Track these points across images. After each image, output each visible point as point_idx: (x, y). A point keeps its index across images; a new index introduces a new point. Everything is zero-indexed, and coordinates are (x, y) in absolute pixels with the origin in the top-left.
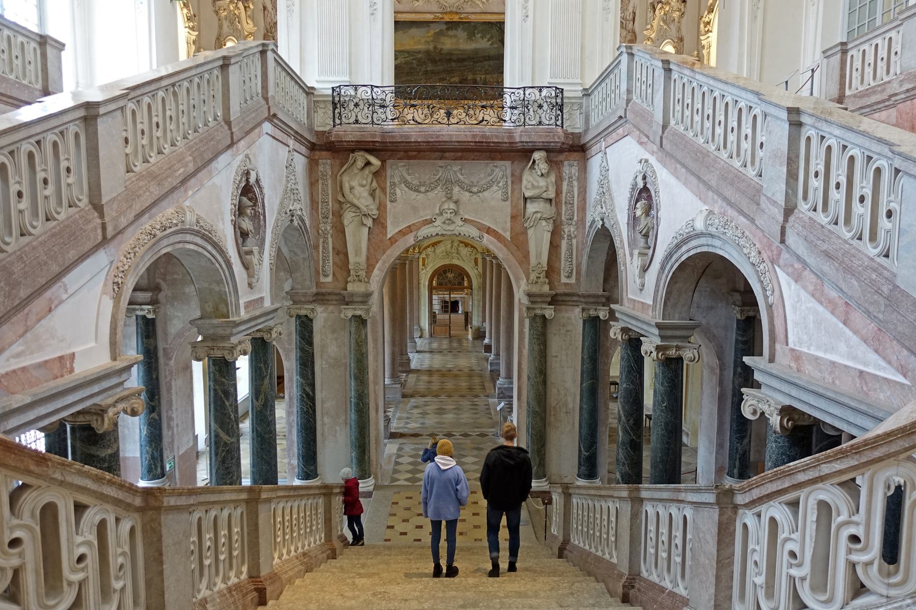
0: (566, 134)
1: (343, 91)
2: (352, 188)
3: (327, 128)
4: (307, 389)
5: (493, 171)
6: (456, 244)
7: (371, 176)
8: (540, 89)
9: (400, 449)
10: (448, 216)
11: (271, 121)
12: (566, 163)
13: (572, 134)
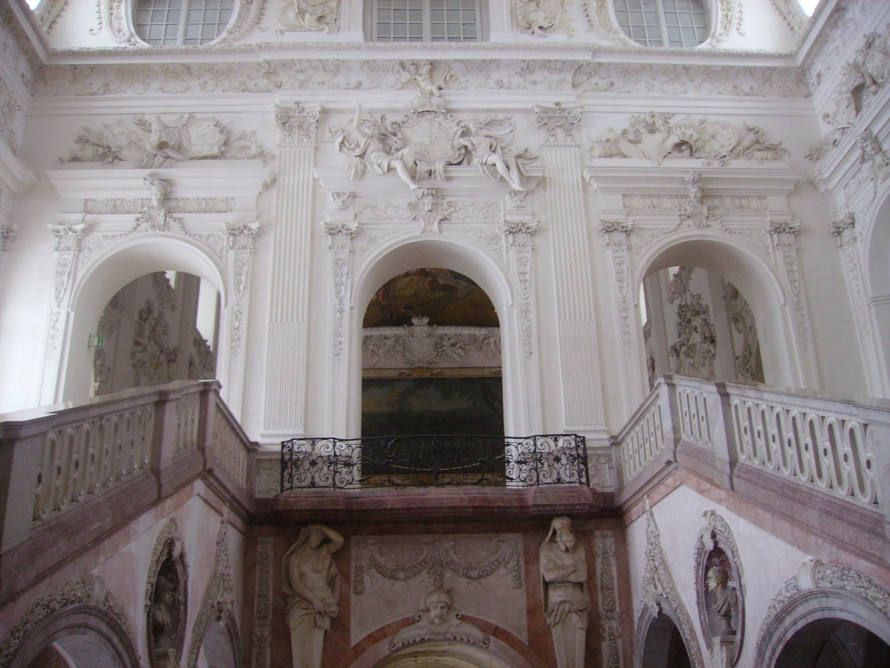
0: (595, 493)
1: (295, 447)
2: (302, 575)
3: (272, 495)
5: (499, 547)
8: (556, 438)
11: (205, 479)
12: (597, 533)
13: (602, 493)
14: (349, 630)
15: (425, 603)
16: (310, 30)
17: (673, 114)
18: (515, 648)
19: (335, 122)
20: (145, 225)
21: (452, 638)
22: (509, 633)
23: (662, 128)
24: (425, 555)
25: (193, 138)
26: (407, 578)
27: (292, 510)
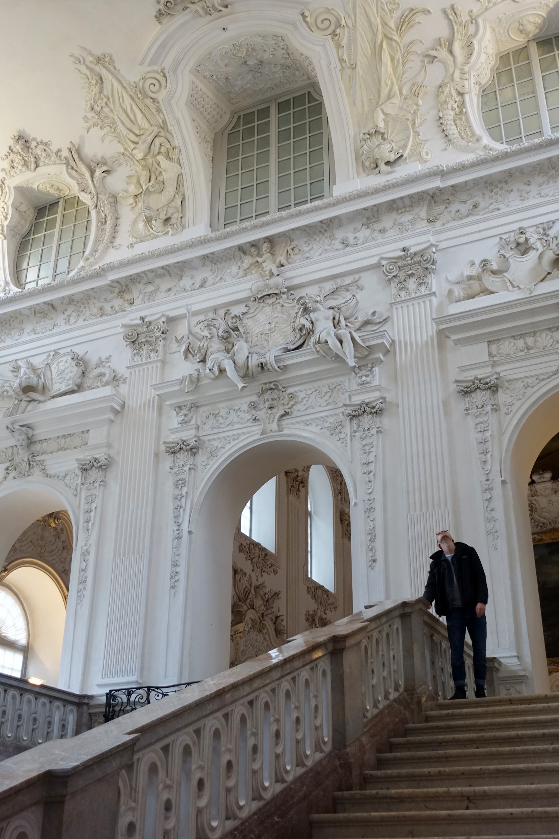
16: (156, 237)
17: (554, 223)
19: (182, 330)
20: (13, 474)
23: (538, 245)
25: (54, 375)
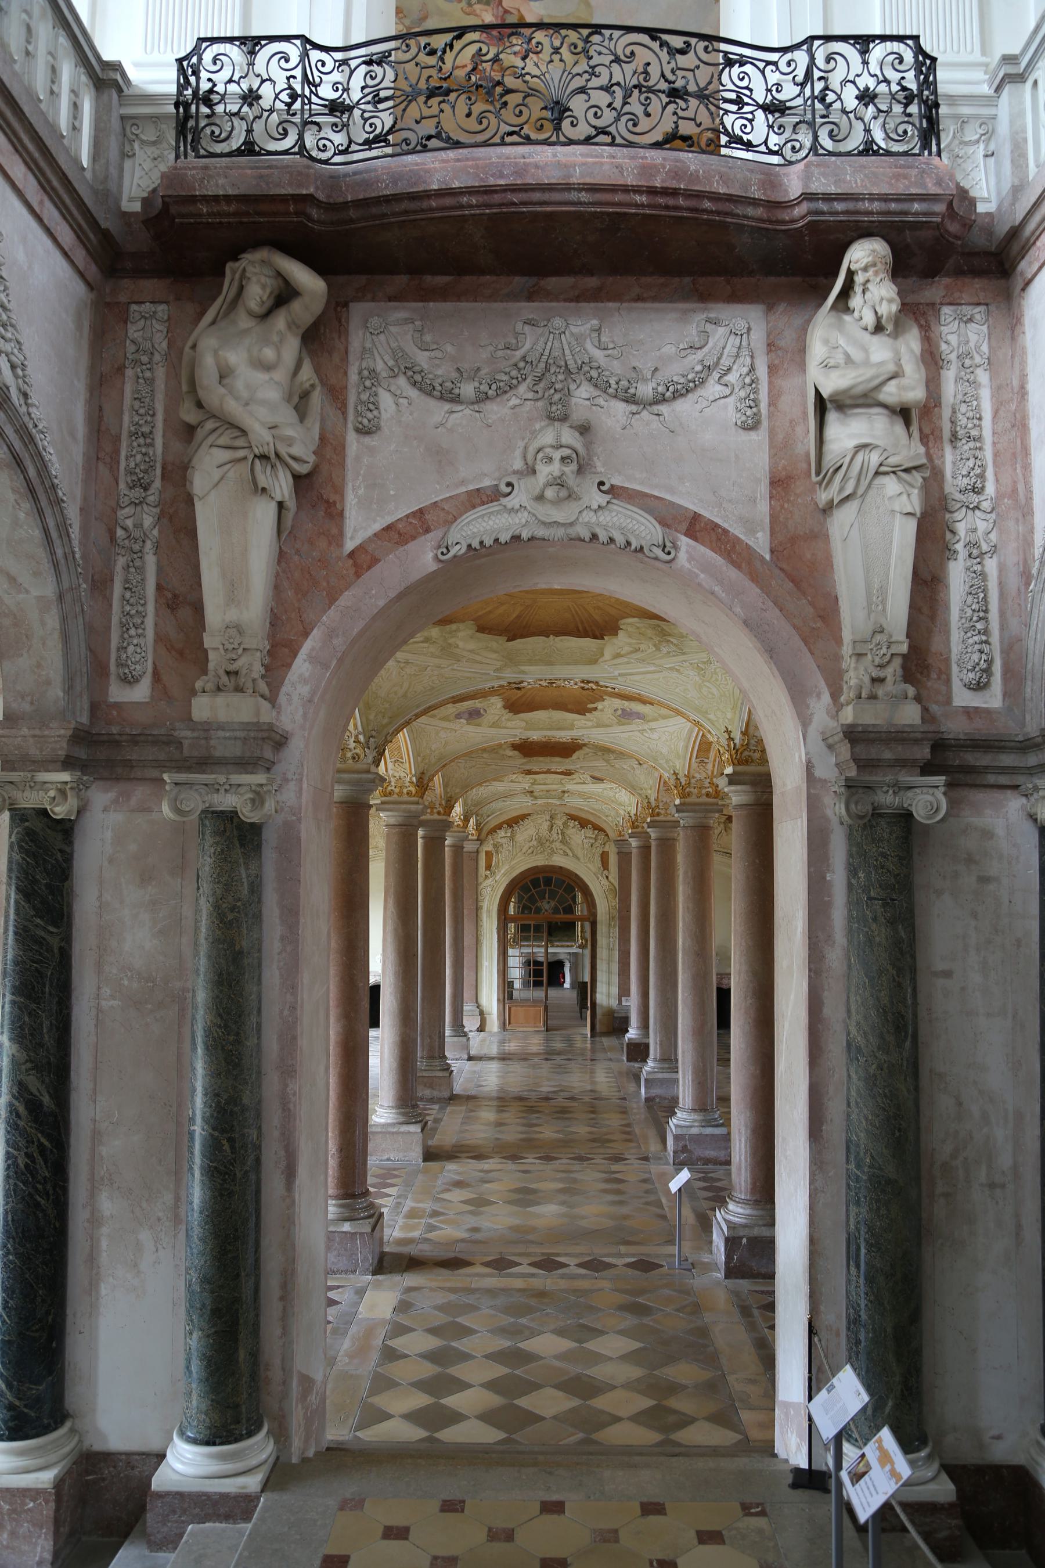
2: (224, 374)
4: (34, 1083)
6: (559, 822)
7: (292, 345)
9: (403, 1307)
10: (556, 468)
12: (946, 310)
14: (341, 514)
15: (525, 458)
18: (738, 567)
21: (587, 536)
22: (725, 531)
24: (528, 346)
26: (482, 398)
27: (193, 199)
